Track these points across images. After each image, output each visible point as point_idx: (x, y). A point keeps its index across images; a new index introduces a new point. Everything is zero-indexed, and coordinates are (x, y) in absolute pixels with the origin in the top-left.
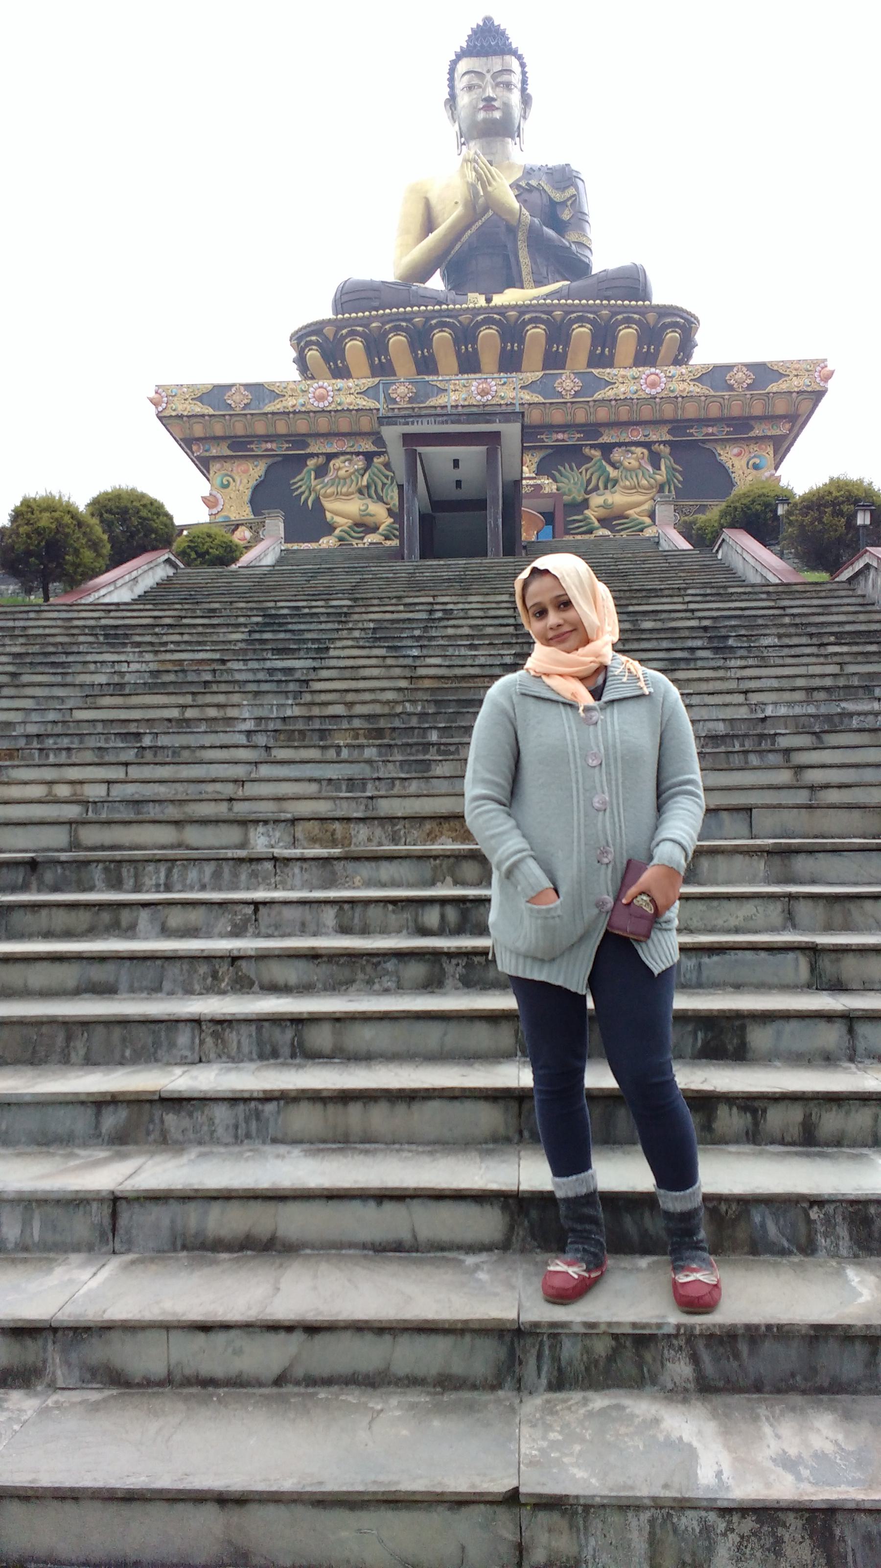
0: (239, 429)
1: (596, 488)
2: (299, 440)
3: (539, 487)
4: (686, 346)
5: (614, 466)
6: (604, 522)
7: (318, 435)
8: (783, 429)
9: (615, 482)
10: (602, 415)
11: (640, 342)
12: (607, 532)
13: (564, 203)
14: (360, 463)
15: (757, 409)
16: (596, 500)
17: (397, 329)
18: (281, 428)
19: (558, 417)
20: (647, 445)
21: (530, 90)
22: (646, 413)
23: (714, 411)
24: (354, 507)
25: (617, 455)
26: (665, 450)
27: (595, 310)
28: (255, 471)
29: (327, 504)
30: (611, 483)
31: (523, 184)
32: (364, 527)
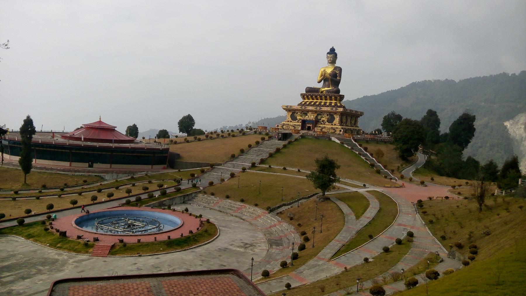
2: (295, 111)
6: (323, 121)
8: (339, 114)
14: (300, 113)
15: (336, 112)
17: (309, 95)
19: (318, 111)
28: (291, 113)
30: (323, 117)
31: (333, 71)
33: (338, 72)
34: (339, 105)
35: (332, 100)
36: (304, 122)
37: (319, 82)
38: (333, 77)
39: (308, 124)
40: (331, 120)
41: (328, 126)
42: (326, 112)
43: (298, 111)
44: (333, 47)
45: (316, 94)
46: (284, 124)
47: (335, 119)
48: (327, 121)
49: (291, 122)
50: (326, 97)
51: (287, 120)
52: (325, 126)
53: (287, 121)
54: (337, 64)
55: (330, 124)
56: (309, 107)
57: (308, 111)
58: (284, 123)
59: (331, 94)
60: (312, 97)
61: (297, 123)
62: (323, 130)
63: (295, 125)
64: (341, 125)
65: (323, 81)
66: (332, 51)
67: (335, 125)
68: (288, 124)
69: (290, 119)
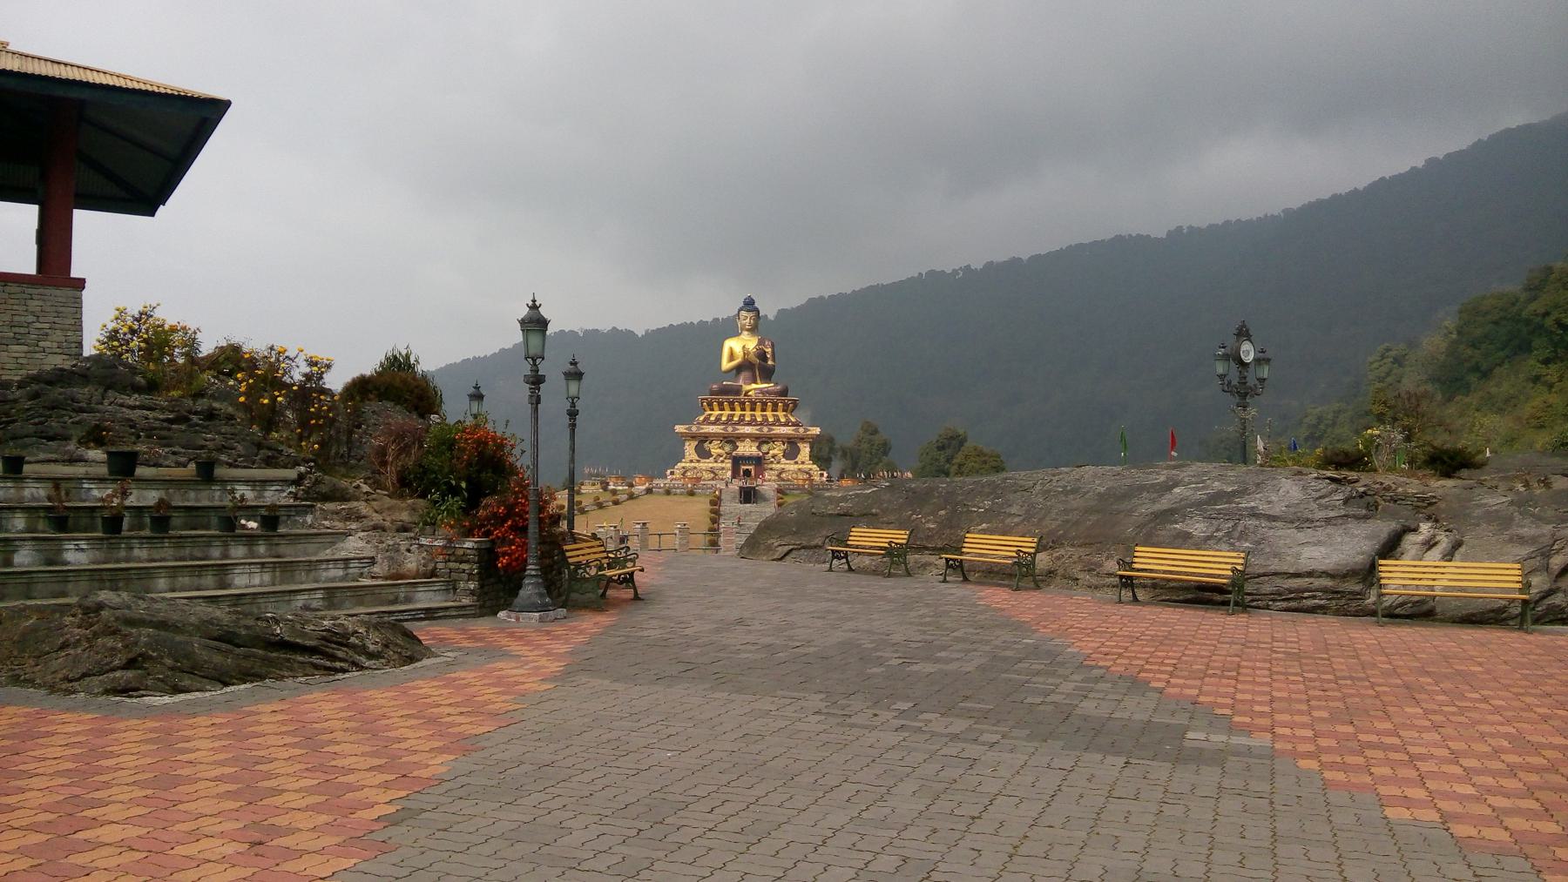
2: (707, 437)
6: (773, 457)
16: (771, 452)
24: (720, 451)
28: (696, 443)
29: (712, 450)
34: (793, 420)
35: (777, 411)
36: (737, 461)
38: (763, 361)
39: (744, 465)
40: (791, 454)
41: (790, 466)
42: (780, 438)
45: (731, 398)
46: (683, 468)
47: (799, 450)
48: (783, 456)
49: (698, 461)
50: (764, 405)
52: (783, 466)
53: (688, 460)
55: (792, 462)
57: (742, 437)
58: (683, 465)
59: (775, 398)
60: (731, 404)
61: (715, 465)
62: (784, 475)
63: (711, 468)
64: (814, 464)
65: (734, 371)
67: (803, 463)
68: (695, 468)
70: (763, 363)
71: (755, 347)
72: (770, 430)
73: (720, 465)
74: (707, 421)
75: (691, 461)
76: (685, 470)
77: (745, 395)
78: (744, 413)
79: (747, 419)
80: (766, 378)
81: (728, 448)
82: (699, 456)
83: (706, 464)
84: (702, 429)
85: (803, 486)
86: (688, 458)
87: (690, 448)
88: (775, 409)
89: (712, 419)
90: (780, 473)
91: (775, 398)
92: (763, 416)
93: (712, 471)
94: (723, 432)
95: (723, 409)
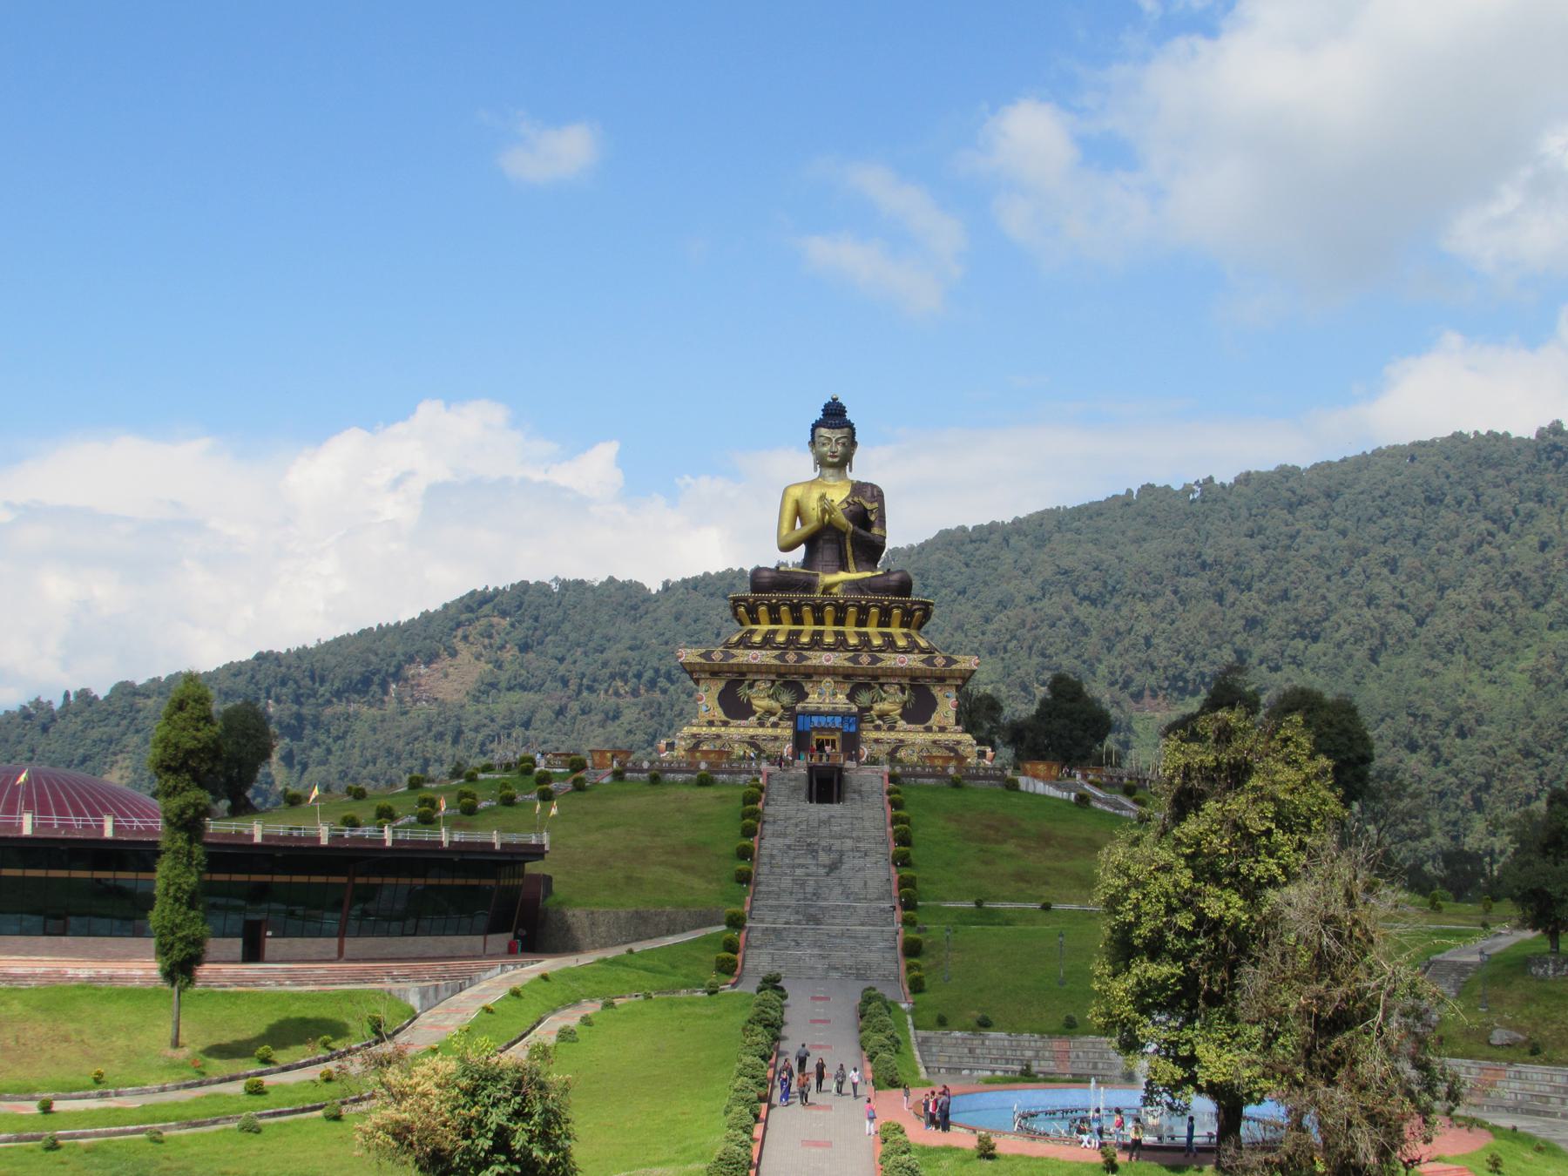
0: (716, 669)
1: (876, 701)
2: (743, 674)
3: (850, 709)
4: (927, 615)
5: (885, 692)
7: (750, 672)
9: (885, 699)
10: (879, 671)
11: (903, 616)
12: (881, 723)
13: (872, 510)
14: (769, 685)
15: (947, 674)
17: (784, 604)
18: (735, 669)
19: (860, 672)
20: (900, 684)
21: (857, 439)
22: (899, 672)
23: (928, 674)
25: (886, 688)
26: (908, 687)
27: (882, 601)
28: (721, 685)
29: (755, 702)
30: (882, 700)
31: (850, 500)
32: (770, 713)
33: (876, 505)
34: (923, 643)
35: (888, 625)
37: (787, 548)
40: (919, 710)
41: (916, 736)
43: (756, 673)
44: (835, 400)
46: (694, 736)
48: (902, 716)
49: (725, 724)
50: (863, 611)
51: (704, 716)
52: (901, 736)
54: (862, 469)
55: (920, 727)
56: (818, 654)
57: (813, 674)
58: (695, 730)
60: (796, 610)
61: (760, 731)
62: (901, 754)
63: (752, 737)
64: (966, 731)
66: (834, 415)
67: (942, 729)
68: (718, 736)
69: (719, 714)
70: (862, 532)
71: (846, 501)
72: (875, 660)
73: (770, 730)
74: (745, 643)
75: (711, 723)
76: (697, 741)
77: (824, 592)
78: (822, 628)
79: (829, 640)
80: (867, 561)
81: (786, 699)
82: (726, 713)
83: (740, 730)
84: (734, 656)
85: (945, 769)
86: (704, 716)
87: (708, 698)
88: (884, 622)
89: (757, 639)
90: (895, 750)
91: (887, 600)
92: (859, 634)
93: (752, 742)
94: (777, 662)
95: (777, 621)
